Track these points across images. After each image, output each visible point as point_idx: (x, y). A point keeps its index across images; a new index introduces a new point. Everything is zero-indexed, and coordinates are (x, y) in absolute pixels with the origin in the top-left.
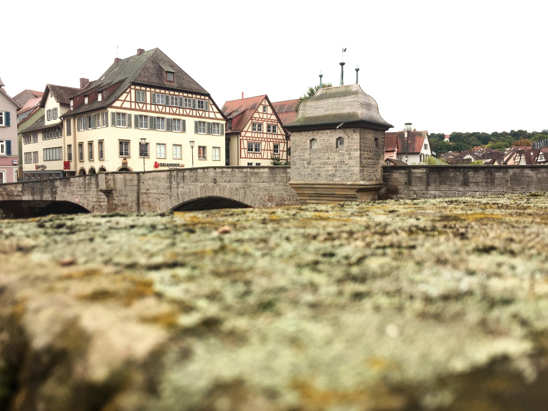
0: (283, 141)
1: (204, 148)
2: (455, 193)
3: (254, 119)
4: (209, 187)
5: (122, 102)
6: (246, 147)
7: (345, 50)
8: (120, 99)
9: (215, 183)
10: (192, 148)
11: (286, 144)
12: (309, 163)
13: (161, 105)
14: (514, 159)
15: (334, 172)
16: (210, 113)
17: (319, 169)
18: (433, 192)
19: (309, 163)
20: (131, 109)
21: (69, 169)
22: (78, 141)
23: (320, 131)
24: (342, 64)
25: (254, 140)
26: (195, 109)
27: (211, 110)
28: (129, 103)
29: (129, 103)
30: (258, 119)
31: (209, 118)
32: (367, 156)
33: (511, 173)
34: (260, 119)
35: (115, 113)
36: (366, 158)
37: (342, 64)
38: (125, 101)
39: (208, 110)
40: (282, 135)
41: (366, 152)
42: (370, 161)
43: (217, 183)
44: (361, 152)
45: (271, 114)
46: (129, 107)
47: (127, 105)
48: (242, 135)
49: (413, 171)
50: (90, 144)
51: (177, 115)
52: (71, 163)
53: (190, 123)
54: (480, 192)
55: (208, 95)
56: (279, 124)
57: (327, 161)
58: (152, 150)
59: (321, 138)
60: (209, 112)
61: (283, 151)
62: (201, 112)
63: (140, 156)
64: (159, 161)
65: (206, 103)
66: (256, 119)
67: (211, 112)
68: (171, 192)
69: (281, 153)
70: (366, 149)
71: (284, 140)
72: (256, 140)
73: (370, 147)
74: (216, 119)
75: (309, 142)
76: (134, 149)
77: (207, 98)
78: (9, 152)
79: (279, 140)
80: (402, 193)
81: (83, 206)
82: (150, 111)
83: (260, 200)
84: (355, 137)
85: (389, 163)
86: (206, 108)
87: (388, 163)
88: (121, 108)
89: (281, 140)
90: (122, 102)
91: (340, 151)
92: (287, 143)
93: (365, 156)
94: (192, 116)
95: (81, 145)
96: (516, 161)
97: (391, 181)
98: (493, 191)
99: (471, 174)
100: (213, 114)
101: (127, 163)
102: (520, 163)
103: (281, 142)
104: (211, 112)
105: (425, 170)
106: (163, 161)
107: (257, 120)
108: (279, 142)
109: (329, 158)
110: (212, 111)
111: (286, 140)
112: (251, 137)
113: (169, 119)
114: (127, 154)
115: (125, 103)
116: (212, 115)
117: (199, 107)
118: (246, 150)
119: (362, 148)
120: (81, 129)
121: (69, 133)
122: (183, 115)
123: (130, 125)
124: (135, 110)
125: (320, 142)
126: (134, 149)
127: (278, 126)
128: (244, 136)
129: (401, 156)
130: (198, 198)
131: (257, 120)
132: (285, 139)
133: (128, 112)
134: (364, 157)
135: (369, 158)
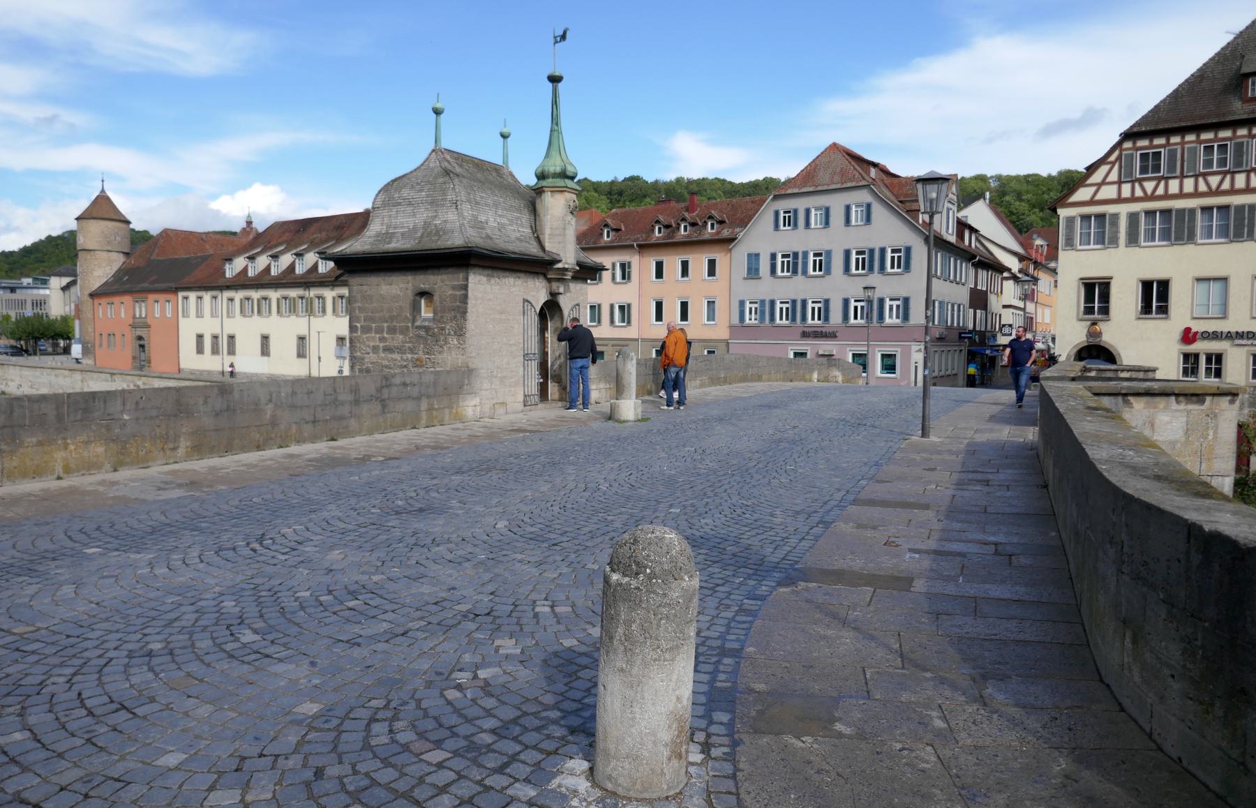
5: (1094, 188)
7: (563, 37)
8: (1090, 181)
20: (1119, 200)
24: (555, 79)
29: (1115, 187)
32: (381, 345)
35: (1074, 217)
36: (375, 349)
37: (555, 79)
38: (1104, 183)
41: (376, 333)
42: (396, 356)
44: (355, 335)
46: (1114, 195)
47: (1109, 192)
58: (1179, 297)
64: (1197, 327)
70: (374, 325)
73: (392, 318)
76: (1125, 298)
78: (906, 317)
82: (1181, 195)
88: (1092, 202)
90: (1094, 188)
93: (372, 344)
106: (1211, 326)
114: (1105, 310)
115: (1104, 188)
119: (359, 325)
123: (1114, 241)
124: (1133, 199)
126: (1125, 298)
133: (1110, 209)
134: (369, 346)
135: (388, 349)
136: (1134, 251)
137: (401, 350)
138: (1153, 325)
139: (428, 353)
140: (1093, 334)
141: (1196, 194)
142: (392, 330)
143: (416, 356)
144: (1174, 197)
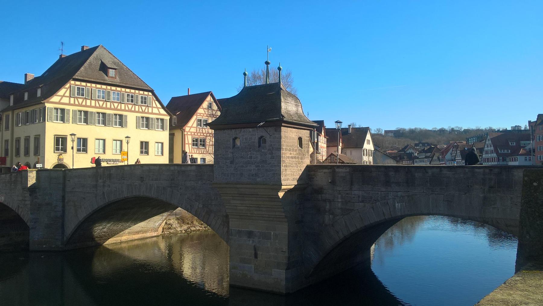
1: (147, 143)
2: (378, 193)
3: (199, 114)
4: (136, 185)
6: (190, 141)
9: (142, 181)
10: (128, 144)
12: (232, 162)
13: (101, 101)
15: (257, 172)
16: (154, 109)
17: (242, 168)
18: (356, 192)
19: (232, 162)
20: (69, 104)
21: (5, 164)
22: (15, 136)
23: (243, 130)
25: (199, 136)
26: (137, 104)
27: (154, 105)
28: (68, 99)
30: (202, 115)
31: (152, 113)
32: (290, 156)
33: (430, 173)
34: (204, 115)
35: (53, 108)
36: (288, 157)
38: (64, 96)
39: (151, 106)
41: (289, 151)
42: (294, 160)
43: (144, 182)
45: (217, 110)
46: (67, 102)
47: (65, 100)
48: (186, 131)
49: (337, 170)
50: (27, 139)
51: (118, 110)
52: (7, 158)
53: (131, 118)
54: (402, 193)
55: (152, 91)
57: (249, 160)
59: (243, 137)
60: (152, 107)
62: (144, 108)
63: (77, 151)
65: (150, 99)
66: (201, 115)
67: (154, 107)
68: (96, 191)
70: (288, 148)
72: (201, 135)
74: (160, 114)
75: (231, 140)
77: (150, 94)
80: (327, 193)
81: (8, 205)
82: (91, 106)
83: (187, 199)
84: (277, 136)
86: (150, 104)
87: (332, 157)
88: (59, 103)
91: (263, 151)
94: (135, 111)
95: (18, 140)
96: (452, 155)
97: (317, 181)
98: (413, 191)
99: (392, 175)
100: (156, 109)
101: (63, 159)
104: (154, 107)
105: (348, 170)
107: (201, 116)
109: (251, 157)
110: (155, 106)
112: (196, 133)
113: (110, 114)
115: (64, 98)
116: (155, 111)
117: (142, 102)
118: (190, 146)
120: (19, 124)
121: (7, 128)
122: (125, 110)
124: (74, 105)
125: (243, 140)
128: (189, 131)
130: (125, 197)
131: (201, 116)
135: (292, 158)
136: (75, 125)
137: (295, 157)
138: (82, 155)
139: (301, 159)
140: (59, 159)
141: (95, 107)
142: (293, 150)
143: (299, 160)
144: (123, 110)
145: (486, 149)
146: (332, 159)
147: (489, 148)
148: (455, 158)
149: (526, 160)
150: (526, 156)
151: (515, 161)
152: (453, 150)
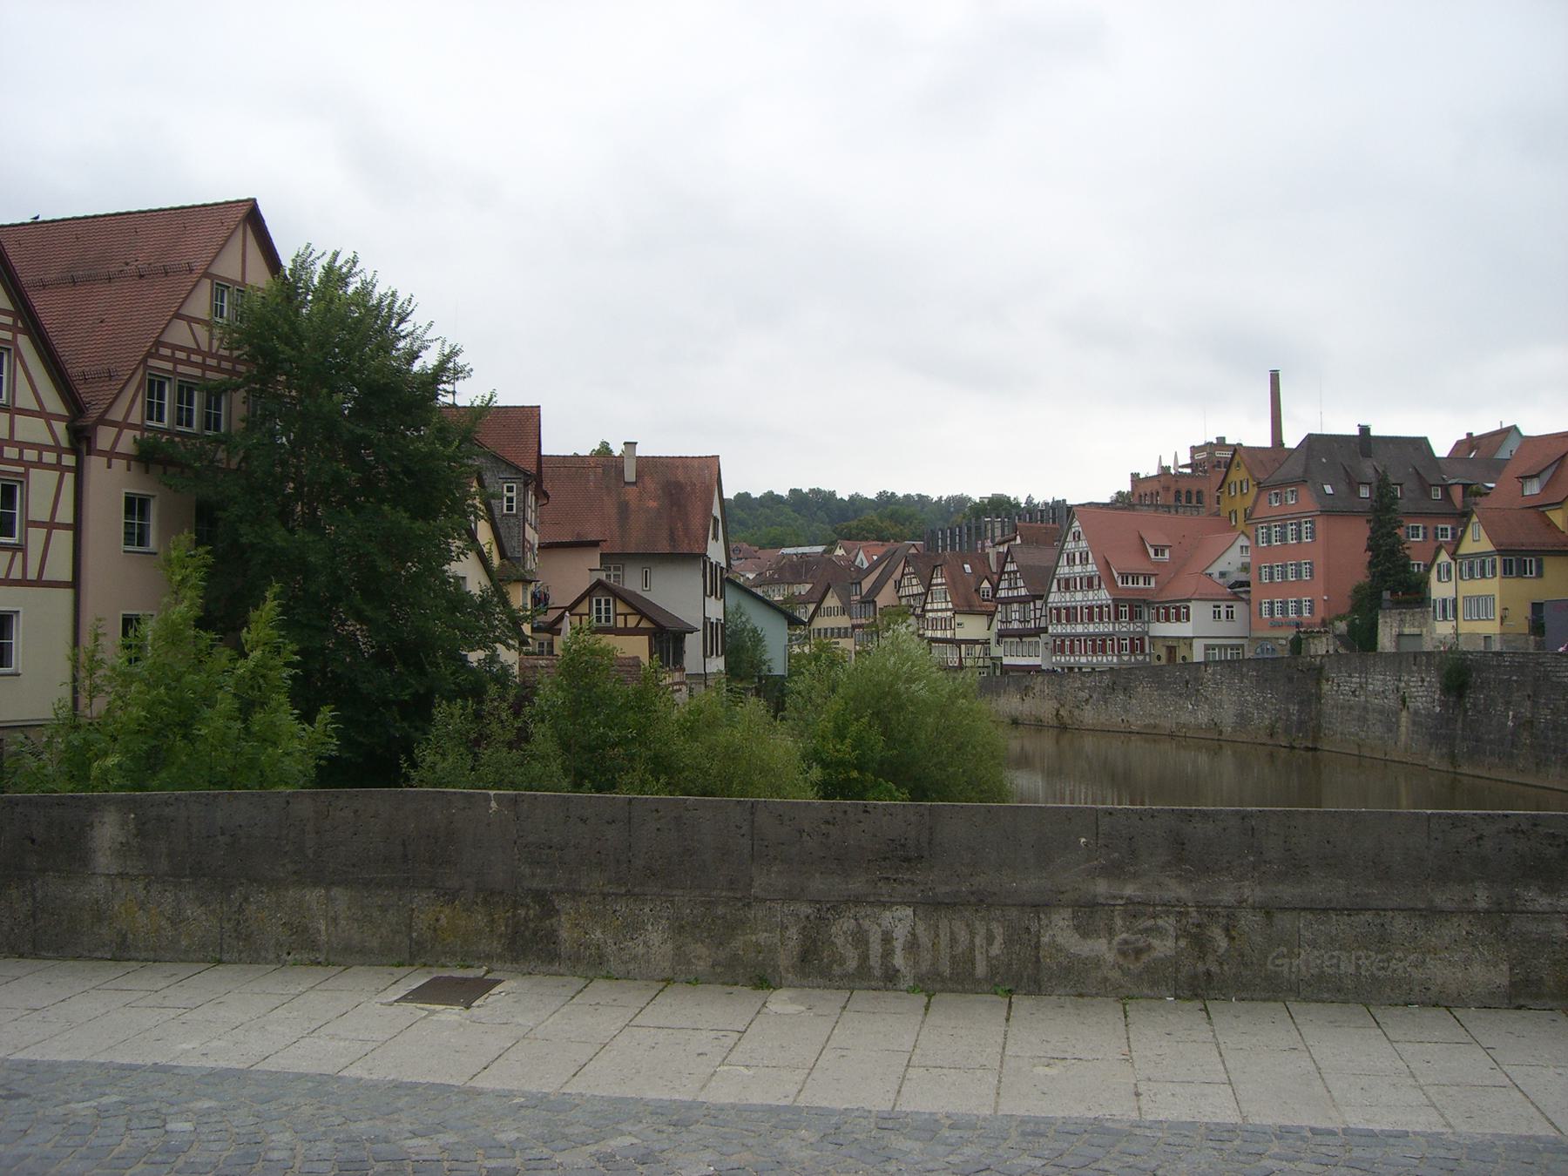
0: (50, 457)
11: (69, 478)
14: (898, 586)
40: (41, 413)
56: (24, 342)
61: (51, 526)
69: (36, 536)
71: (57, 449)
79: (23, 446)
85: (607, 602)
87: (598, 602)
89: (41, 448)
92: (79, 472)
96: (902, 592)
102: (929, 600)
103: (40, 464)
108: (19, 461)
111: (74, 450)
127: (19, 354)
129: (615, 569)
132: (64, 443)
145: (1064, 570)
146: (598, 611)
147: (1078, 569)
148: (925, 603)
149: (1217, 615)
150: (1230, 603)
151: (1178, 619)
152: (907, 570)
